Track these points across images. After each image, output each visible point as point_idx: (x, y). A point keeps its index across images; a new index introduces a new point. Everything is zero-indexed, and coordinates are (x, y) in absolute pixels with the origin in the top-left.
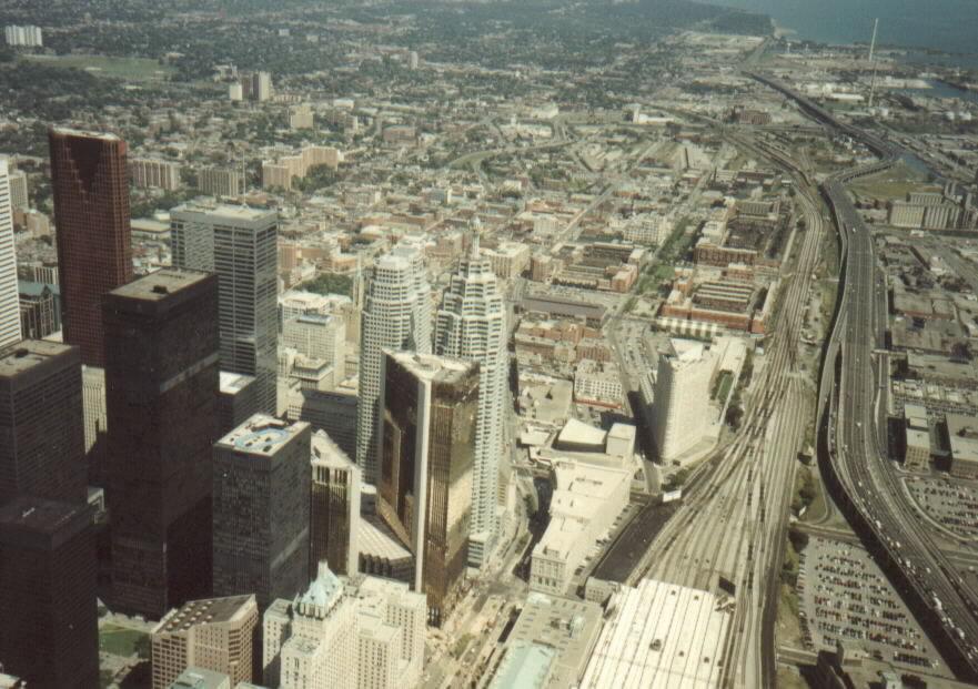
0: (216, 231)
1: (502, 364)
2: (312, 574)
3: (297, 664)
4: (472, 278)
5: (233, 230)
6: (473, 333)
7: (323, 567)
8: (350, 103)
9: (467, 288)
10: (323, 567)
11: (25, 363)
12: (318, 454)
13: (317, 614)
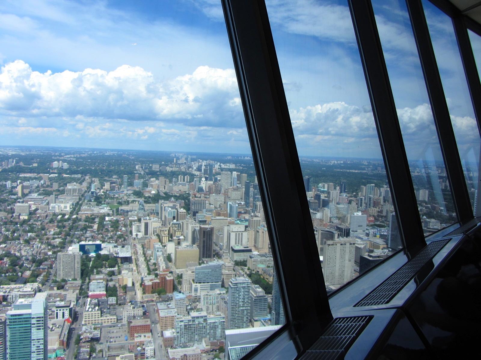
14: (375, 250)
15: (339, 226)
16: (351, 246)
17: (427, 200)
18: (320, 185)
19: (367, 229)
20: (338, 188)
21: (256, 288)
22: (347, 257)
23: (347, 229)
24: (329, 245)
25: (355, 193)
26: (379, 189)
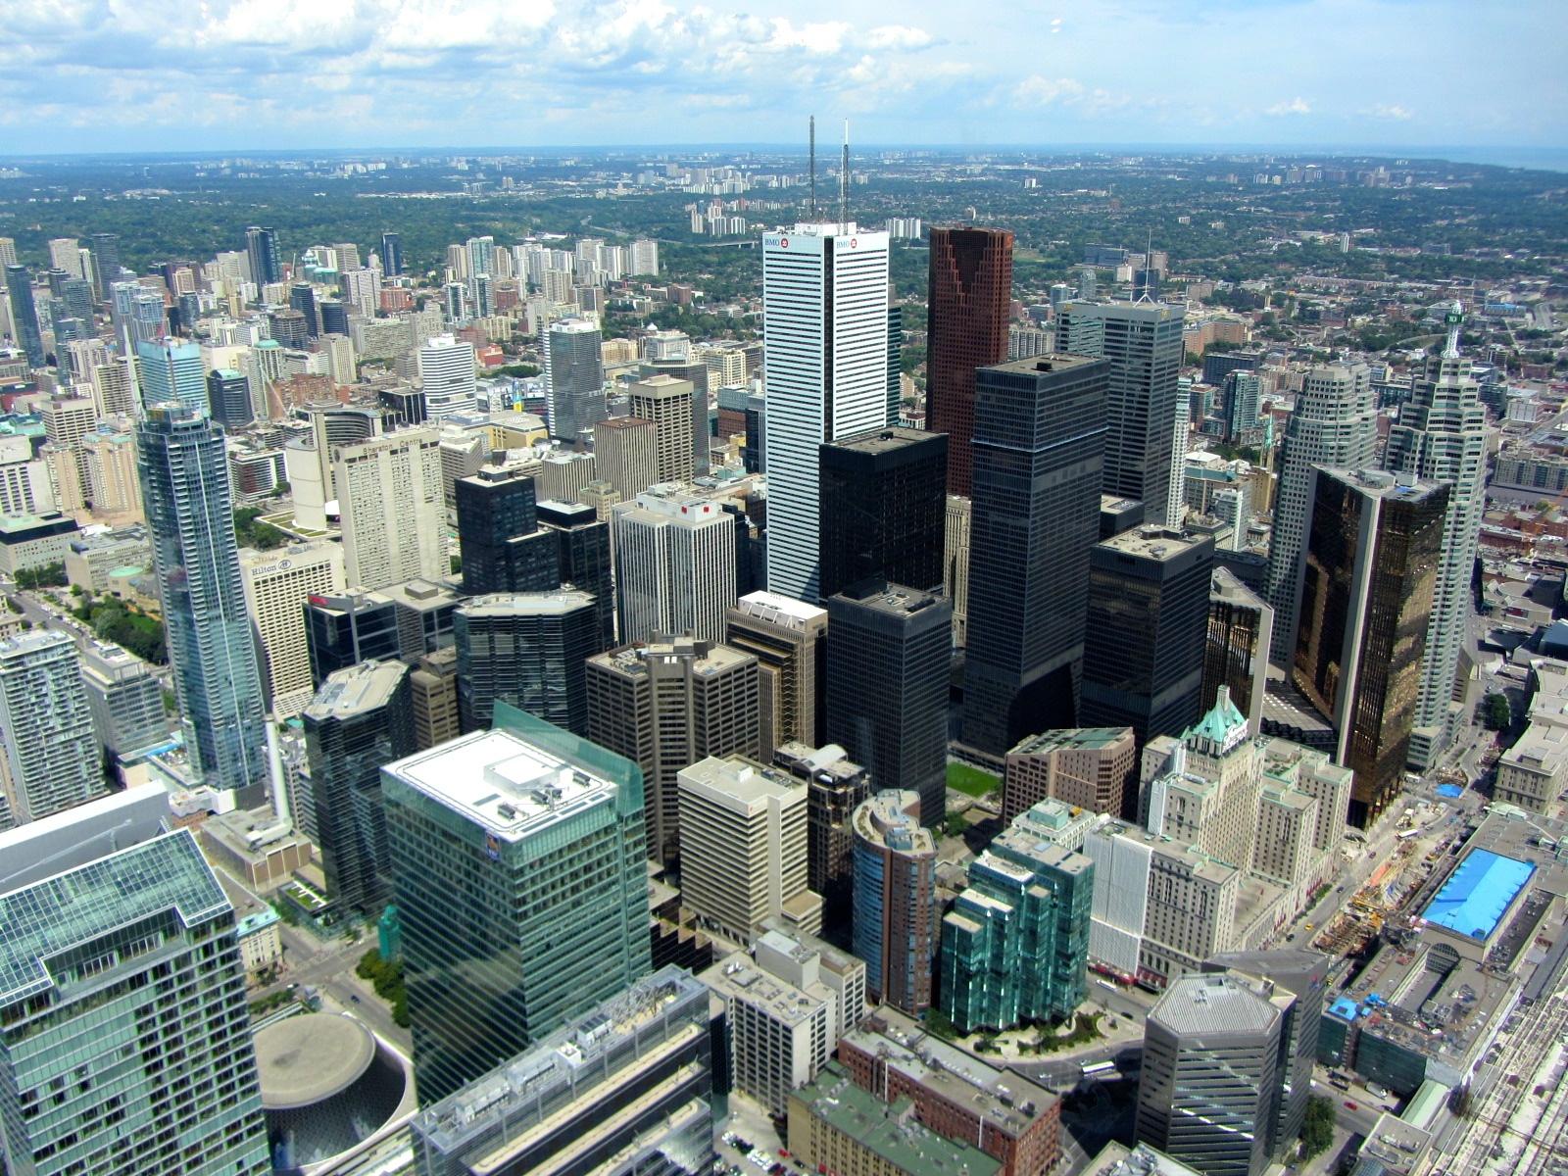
0: (1108, 326)
1: (1478, 503)
2: (1210, 704)
3: (1183, 801)
4: (1444, 381)
5: (1130, 324)
6: (1441, 454)
7: (1224, 692)
8: (1261, 286)
9: (1436, 394)
10: (1224, 692)
11: (890, 445)
12: (1218, 589)
13: (1212, 751)
14: (510, 453)
15: (390, 391)
16: (425, 451)
17: (655, 272)
18: (309, 253)
19: (480, 389)
20: (374, 259)
21: (108, 654)
22: (419, 491)
23: (415, 396)
24: (353, 460)
25: (432, 273)
26: (510, 250)
